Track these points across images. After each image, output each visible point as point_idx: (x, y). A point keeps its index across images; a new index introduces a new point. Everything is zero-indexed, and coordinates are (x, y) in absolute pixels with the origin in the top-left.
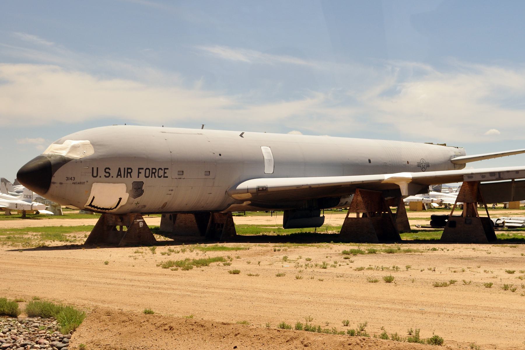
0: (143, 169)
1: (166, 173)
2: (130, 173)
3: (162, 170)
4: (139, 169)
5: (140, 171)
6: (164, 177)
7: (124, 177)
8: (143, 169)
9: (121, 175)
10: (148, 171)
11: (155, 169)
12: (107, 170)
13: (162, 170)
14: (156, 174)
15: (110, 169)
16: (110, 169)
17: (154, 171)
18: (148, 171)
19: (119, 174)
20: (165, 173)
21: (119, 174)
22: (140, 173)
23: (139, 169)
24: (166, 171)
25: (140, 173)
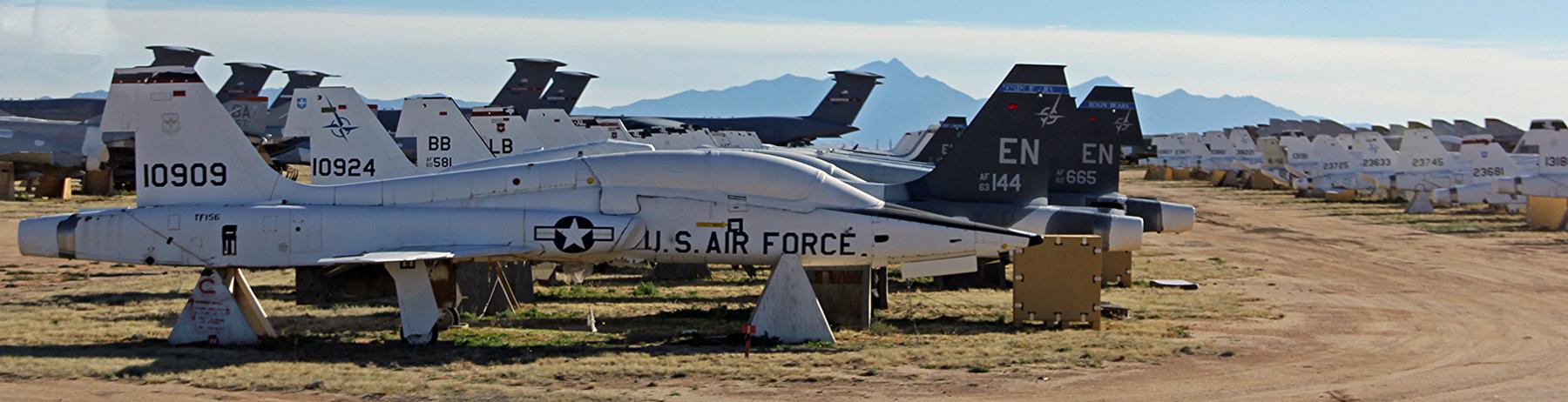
0: (777, 234)
1: (848, 245)
2: (742, 244)
3: (834, 237)
4: (766, 235)
5: (770, 239)
6: (842, 253)
7: (727, 251)
8: (777, 234)
9: (717, 248)
10: (791, 240)
11: (812, 235)
12: (683, 238)
13: (834, 237)
14: (817, 247)
15: (689, 235)
16: (689, 235)
17: (810, 240)
18: (791, 240)
19: (714, 245)
20: (843, 245)
21: (714, 245)
22: (771, 244)
23: (766, 235)
24: (846, 240)
25: (771, 244)
